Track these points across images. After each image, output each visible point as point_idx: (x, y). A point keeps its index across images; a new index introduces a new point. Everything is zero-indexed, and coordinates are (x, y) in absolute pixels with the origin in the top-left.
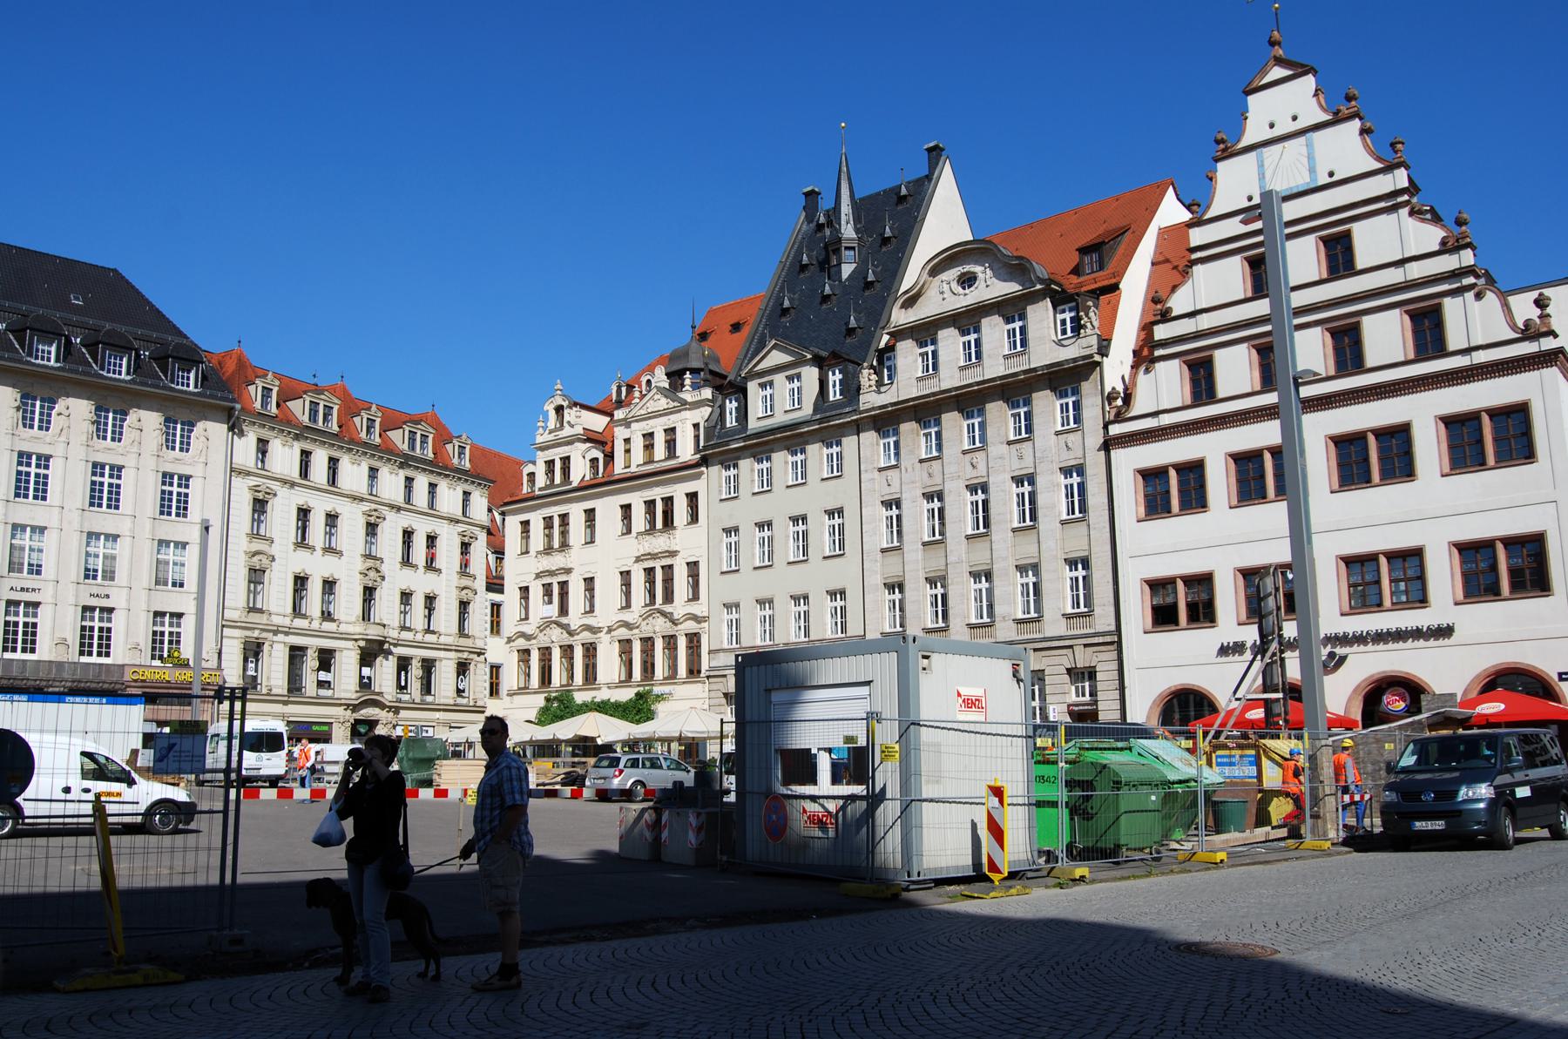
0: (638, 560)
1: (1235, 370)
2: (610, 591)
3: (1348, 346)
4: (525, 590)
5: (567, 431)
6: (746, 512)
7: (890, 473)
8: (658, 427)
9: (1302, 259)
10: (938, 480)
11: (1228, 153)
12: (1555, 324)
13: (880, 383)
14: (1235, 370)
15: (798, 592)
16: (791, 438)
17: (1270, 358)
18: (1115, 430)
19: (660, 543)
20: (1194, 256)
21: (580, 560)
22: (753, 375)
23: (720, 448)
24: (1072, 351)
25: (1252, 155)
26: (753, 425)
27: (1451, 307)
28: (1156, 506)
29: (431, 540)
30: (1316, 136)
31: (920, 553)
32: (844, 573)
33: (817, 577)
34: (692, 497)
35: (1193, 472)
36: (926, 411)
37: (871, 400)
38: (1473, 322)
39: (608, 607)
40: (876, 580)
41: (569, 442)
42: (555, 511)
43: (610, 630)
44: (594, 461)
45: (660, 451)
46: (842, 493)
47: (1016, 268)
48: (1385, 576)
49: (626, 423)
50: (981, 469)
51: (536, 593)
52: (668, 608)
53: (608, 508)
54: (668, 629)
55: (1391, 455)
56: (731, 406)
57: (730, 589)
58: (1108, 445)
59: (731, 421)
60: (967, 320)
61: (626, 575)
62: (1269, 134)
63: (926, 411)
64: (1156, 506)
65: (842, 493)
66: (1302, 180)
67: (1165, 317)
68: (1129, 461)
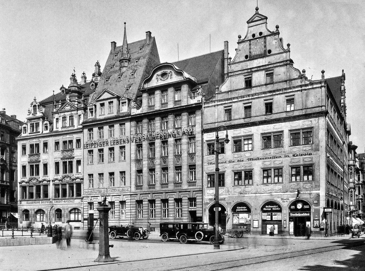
0: (62, 159)
2: (51, 169)
4: (24, 167)
8: (68, 114)
39: (52, 174)
43: (53, 181)
53: (51, 141)
54: (71, 182)
60: (164, 89)
61: (57, 164)
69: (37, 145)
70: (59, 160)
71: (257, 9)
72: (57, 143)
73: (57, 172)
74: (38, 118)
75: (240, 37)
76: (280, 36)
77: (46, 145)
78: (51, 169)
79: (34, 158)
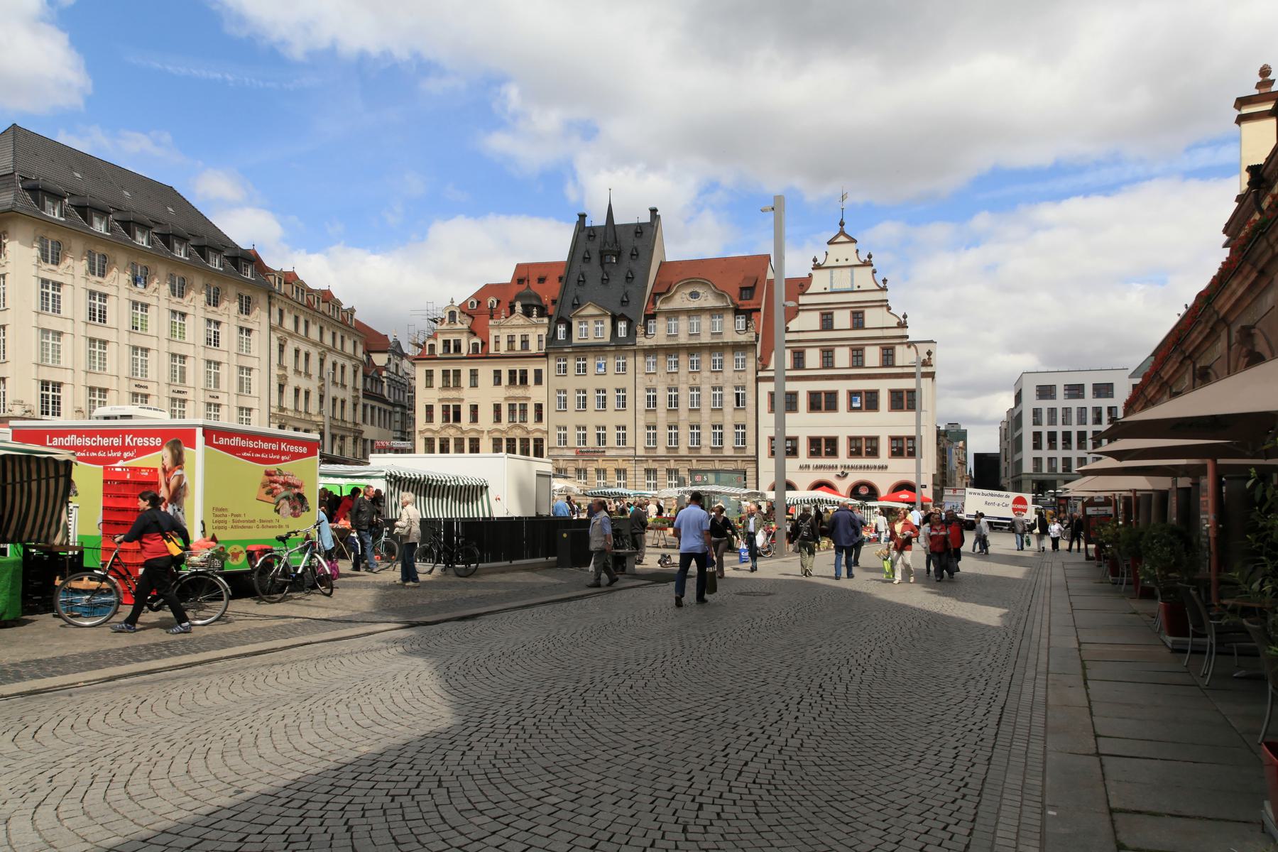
0: (506, 399)
1: (813, 358)
2: (486, 415)
3: (858, 356)
4: (429, 409)
5: (459, 326)
6: (572, 382)
9: (842, 319)
13: (646, 333)
14: (813, 358)
16: (598, 349)
17: (828, 357)
18: (760, 374)
19: (518, 392)
21: (467, 396)
24: (742, 338)
25: (828, 271)
26: (575, 340)
27: (898, 348)
29: (343, 367)
30: (856, 270)
32: (626, 418)
33: (611, 418)
34: (538, 374)
36: (671, 350)
37: (642, 341)
38: (904, 356)
40: (641, 423)
41: (460, 331)
42: (451, 368)
44: (475, 345)
45: (518, 346)
46: (626, 381)
47: (720, 295)
48: (864, 447)
49: (499, 327)
50: (698, 381)
52: (524, 425)
53: (486, 372)
54: (524, 436)
55: (870, 401)
56: (561, 329)
57: (561, 419)
58: (758, 380)
59: (561, 337)
61: (497, 408)
62: (835, 264)
63: (671, 350)
65: (626, 381)
66: (847, 286)
68: (766, 388)
69: (457, 373)
70: (500, 400)
71: (842, 224)
72: (497, 374)
73: (498, 419)
74: (460, 331)
75: (815, 260)
77: (474, 374)
78: (486, 415)
79: (452, 394)
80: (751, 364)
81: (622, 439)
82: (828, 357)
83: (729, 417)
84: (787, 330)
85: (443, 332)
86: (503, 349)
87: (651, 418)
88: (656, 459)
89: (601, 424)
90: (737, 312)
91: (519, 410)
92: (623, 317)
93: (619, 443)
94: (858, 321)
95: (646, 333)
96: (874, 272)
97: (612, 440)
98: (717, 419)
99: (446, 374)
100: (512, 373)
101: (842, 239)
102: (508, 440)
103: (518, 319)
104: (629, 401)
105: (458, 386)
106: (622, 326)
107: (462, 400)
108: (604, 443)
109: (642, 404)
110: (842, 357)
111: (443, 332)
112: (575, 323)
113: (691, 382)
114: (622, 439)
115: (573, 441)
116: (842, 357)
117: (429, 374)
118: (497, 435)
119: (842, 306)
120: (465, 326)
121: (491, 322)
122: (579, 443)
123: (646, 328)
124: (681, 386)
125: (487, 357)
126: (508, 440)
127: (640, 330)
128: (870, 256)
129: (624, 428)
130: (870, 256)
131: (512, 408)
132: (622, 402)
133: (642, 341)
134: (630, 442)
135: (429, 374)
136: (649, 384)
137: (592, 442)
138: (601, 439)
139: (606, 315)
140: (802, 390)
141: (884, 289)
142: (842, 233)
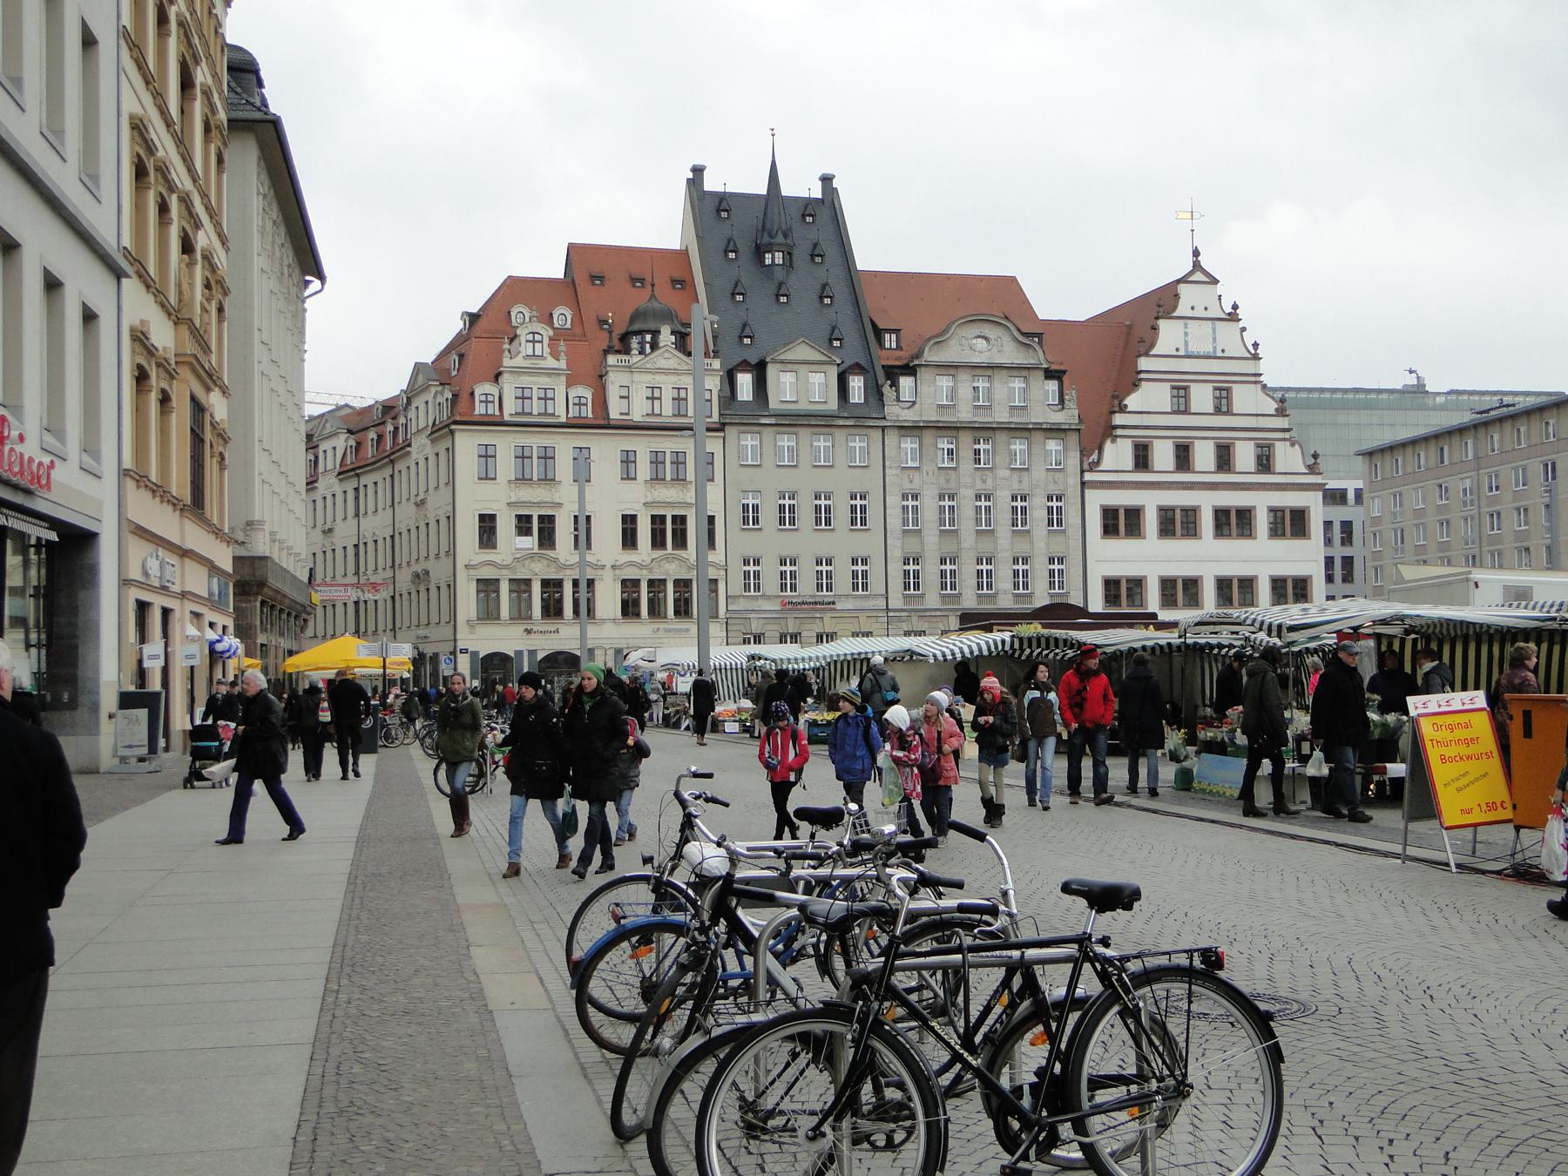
1: (1163, 455)
2: (607, 534)
5: (550, 362)
7: (911, 473)
8: (668, 385)
9: (1202, 397)
10: (953, 484)
11: (1168, 315)
12: (1322, 467)
14: (1163, 455)
15: (825, 554)
18: (1088, 477)
20: (1143, 376)
22: (775, 361)
23: (733, 415)
24: (1058, 418)
26: (773, 404)
28: (1110, 529)
31: (936, 539)
32: (869, 543)
33: (842, 543)
35: (1134, 514)
38: (1288, 459)
40: (896, 553)
41: (552, 373)
45: (667, 408)
49: (630, 369)
50: (989, 481)
51: (505, 526)
53: (605, 450)
56: (745, 381)
58: (1083, 484)
61: (629, 522)
64: (1110, 529)
66: (1208, 349)
67: (1123, 409)
71: (1196, 253)
72: (628, 460)
73: (629, 539)
74: (552, 373)
76: (1241, 324)
80: (1073, 460)
81: (860, 582)
82: (1183, 456)
83: (1041, 543)
84: (1123, 409)
85: (518, 371)
86: (638, 414)
87: (913, 546)
88: (923, 613)
89: (824, 553)
90: (1050, 374)
91: (669, 531)
92: (857, 368)
93: (855, 587)
94: (1223, 403)
95: (898, 399)
96: (1243, 329)
97: (843, 582)
98: (1022, 548)
99: (522, 456)
100: (657, 460)
101: (1198, 276)
102: (651, 583)
103: (667, 356)
104: (874, 515)
105: (548, 479)
106: (856, 384)
107: (560, 505)
108: (830, 588)
109: (895, 522)
110: (1204, 456)
111: (518, 371)
112: (772, 371)
113: (979, 485)
114: (860, 582)
115: (770, 583)
116: (1204, 456)
117: (487, 455)
118: (631, 574)
119: (1202, 377)
120: (563, 364)
121: (612, 359)
122: (783, 587)
123: (897, 391)
124: (963, 491)
125: (602, 423)
126: (651, 583)
127: (887, 390)
128: (1235, 307)
129: (865, 561)
130: (1235, 307)
131: (658, 520)
132: (858, 517)
133: (894, 412)
134: (876, 584)
135: (487, 455)
136: (907, 487)
137: (806, 587)
138: (825, 581)
139: (831, 363)
140: (1151, 503)
141: (1256, 357)
142: (1197, 266)
